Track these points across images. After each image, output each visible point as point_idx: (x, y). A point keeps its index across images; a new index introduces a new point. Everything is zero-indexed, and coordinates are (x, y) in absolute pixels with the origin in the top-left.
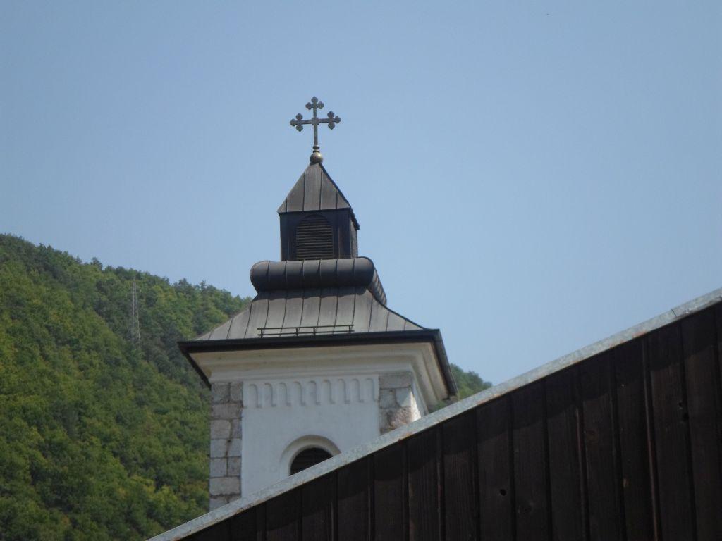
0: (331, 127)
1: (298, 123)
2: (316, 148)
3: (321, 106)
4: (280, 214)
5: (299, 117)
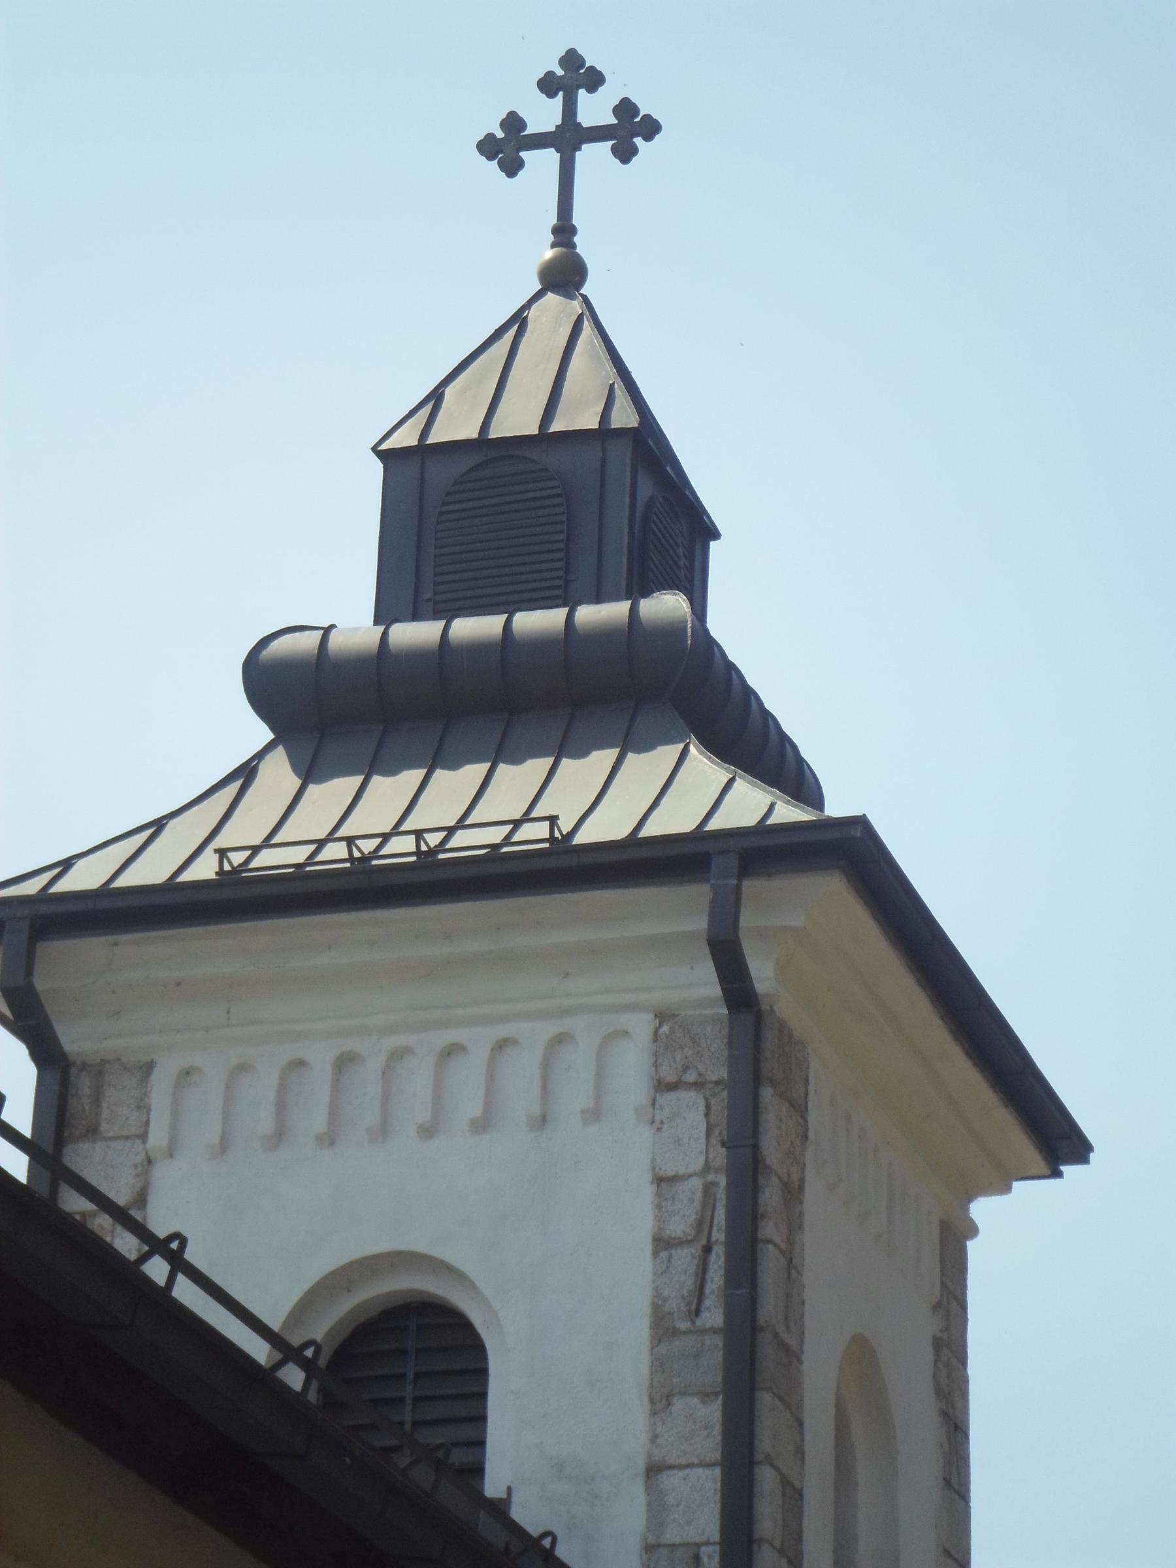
0: (625, 153)
3: (594, 80)
4: (388, 457)
5: (513, 123)
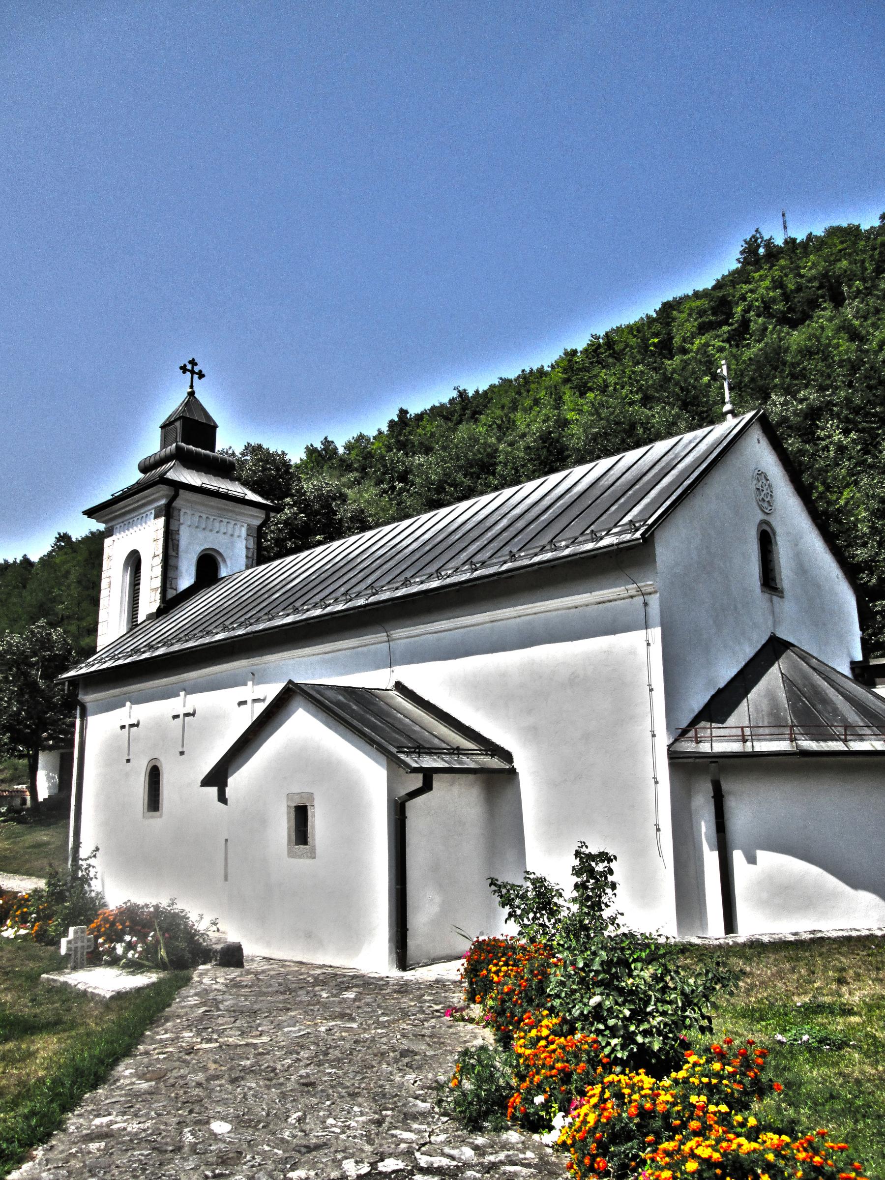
0: (200, 378)
1: (184, 369)
2: (192, 387)
5: (185, 365)
